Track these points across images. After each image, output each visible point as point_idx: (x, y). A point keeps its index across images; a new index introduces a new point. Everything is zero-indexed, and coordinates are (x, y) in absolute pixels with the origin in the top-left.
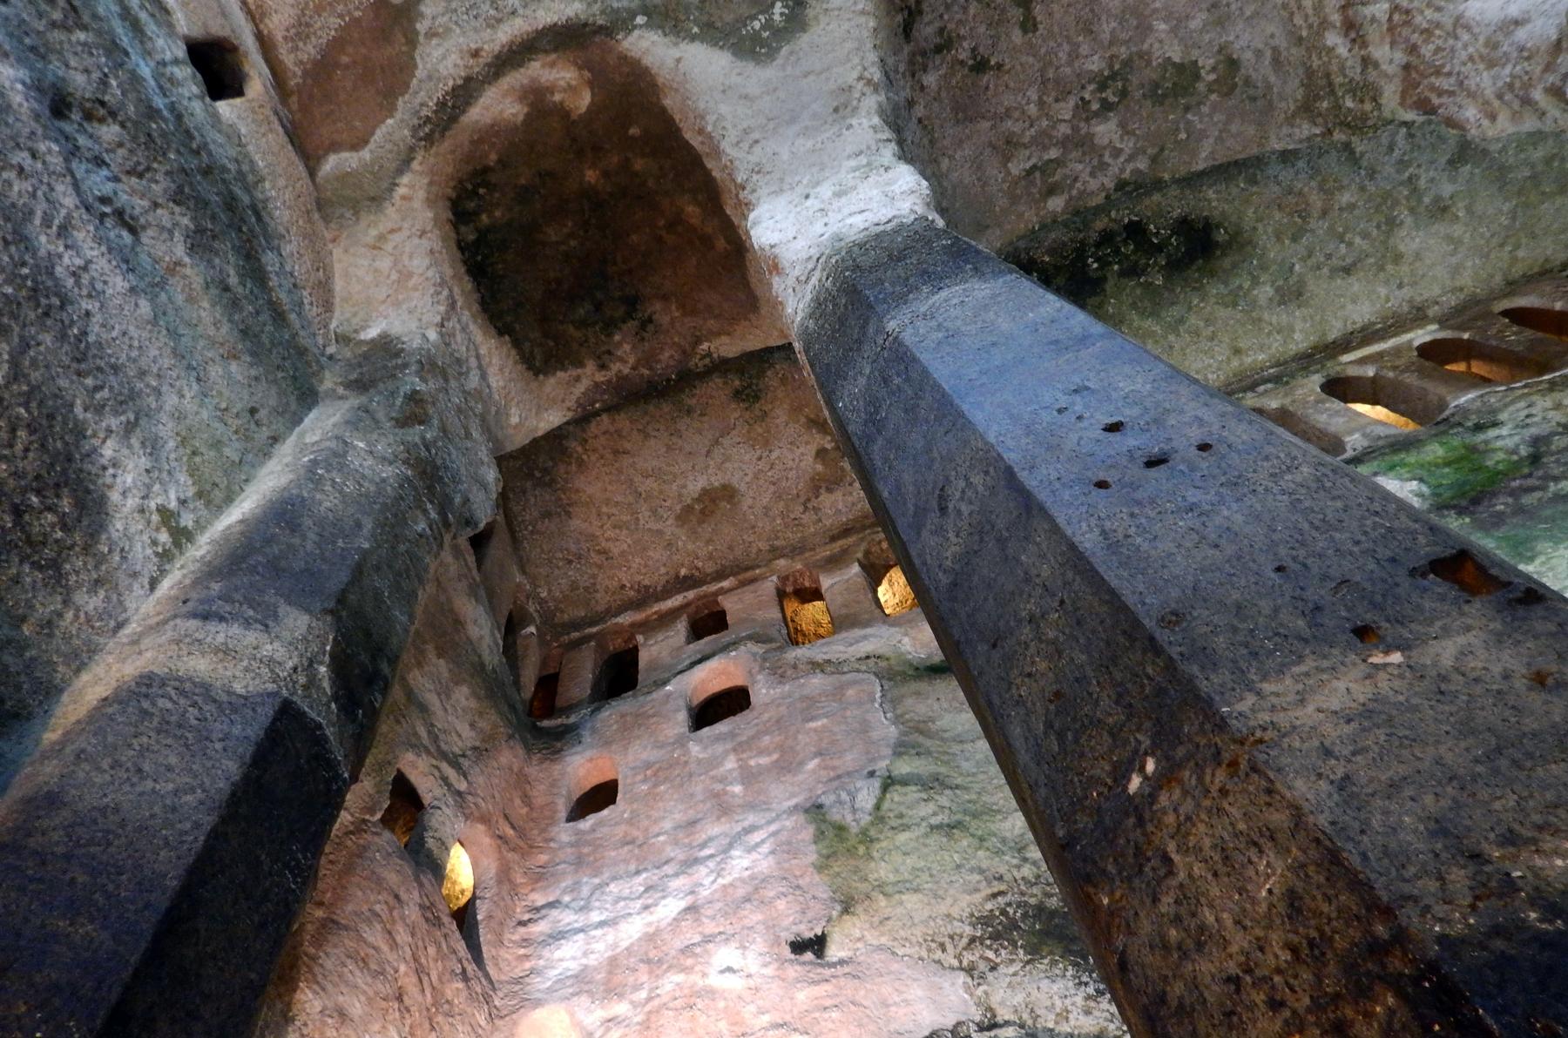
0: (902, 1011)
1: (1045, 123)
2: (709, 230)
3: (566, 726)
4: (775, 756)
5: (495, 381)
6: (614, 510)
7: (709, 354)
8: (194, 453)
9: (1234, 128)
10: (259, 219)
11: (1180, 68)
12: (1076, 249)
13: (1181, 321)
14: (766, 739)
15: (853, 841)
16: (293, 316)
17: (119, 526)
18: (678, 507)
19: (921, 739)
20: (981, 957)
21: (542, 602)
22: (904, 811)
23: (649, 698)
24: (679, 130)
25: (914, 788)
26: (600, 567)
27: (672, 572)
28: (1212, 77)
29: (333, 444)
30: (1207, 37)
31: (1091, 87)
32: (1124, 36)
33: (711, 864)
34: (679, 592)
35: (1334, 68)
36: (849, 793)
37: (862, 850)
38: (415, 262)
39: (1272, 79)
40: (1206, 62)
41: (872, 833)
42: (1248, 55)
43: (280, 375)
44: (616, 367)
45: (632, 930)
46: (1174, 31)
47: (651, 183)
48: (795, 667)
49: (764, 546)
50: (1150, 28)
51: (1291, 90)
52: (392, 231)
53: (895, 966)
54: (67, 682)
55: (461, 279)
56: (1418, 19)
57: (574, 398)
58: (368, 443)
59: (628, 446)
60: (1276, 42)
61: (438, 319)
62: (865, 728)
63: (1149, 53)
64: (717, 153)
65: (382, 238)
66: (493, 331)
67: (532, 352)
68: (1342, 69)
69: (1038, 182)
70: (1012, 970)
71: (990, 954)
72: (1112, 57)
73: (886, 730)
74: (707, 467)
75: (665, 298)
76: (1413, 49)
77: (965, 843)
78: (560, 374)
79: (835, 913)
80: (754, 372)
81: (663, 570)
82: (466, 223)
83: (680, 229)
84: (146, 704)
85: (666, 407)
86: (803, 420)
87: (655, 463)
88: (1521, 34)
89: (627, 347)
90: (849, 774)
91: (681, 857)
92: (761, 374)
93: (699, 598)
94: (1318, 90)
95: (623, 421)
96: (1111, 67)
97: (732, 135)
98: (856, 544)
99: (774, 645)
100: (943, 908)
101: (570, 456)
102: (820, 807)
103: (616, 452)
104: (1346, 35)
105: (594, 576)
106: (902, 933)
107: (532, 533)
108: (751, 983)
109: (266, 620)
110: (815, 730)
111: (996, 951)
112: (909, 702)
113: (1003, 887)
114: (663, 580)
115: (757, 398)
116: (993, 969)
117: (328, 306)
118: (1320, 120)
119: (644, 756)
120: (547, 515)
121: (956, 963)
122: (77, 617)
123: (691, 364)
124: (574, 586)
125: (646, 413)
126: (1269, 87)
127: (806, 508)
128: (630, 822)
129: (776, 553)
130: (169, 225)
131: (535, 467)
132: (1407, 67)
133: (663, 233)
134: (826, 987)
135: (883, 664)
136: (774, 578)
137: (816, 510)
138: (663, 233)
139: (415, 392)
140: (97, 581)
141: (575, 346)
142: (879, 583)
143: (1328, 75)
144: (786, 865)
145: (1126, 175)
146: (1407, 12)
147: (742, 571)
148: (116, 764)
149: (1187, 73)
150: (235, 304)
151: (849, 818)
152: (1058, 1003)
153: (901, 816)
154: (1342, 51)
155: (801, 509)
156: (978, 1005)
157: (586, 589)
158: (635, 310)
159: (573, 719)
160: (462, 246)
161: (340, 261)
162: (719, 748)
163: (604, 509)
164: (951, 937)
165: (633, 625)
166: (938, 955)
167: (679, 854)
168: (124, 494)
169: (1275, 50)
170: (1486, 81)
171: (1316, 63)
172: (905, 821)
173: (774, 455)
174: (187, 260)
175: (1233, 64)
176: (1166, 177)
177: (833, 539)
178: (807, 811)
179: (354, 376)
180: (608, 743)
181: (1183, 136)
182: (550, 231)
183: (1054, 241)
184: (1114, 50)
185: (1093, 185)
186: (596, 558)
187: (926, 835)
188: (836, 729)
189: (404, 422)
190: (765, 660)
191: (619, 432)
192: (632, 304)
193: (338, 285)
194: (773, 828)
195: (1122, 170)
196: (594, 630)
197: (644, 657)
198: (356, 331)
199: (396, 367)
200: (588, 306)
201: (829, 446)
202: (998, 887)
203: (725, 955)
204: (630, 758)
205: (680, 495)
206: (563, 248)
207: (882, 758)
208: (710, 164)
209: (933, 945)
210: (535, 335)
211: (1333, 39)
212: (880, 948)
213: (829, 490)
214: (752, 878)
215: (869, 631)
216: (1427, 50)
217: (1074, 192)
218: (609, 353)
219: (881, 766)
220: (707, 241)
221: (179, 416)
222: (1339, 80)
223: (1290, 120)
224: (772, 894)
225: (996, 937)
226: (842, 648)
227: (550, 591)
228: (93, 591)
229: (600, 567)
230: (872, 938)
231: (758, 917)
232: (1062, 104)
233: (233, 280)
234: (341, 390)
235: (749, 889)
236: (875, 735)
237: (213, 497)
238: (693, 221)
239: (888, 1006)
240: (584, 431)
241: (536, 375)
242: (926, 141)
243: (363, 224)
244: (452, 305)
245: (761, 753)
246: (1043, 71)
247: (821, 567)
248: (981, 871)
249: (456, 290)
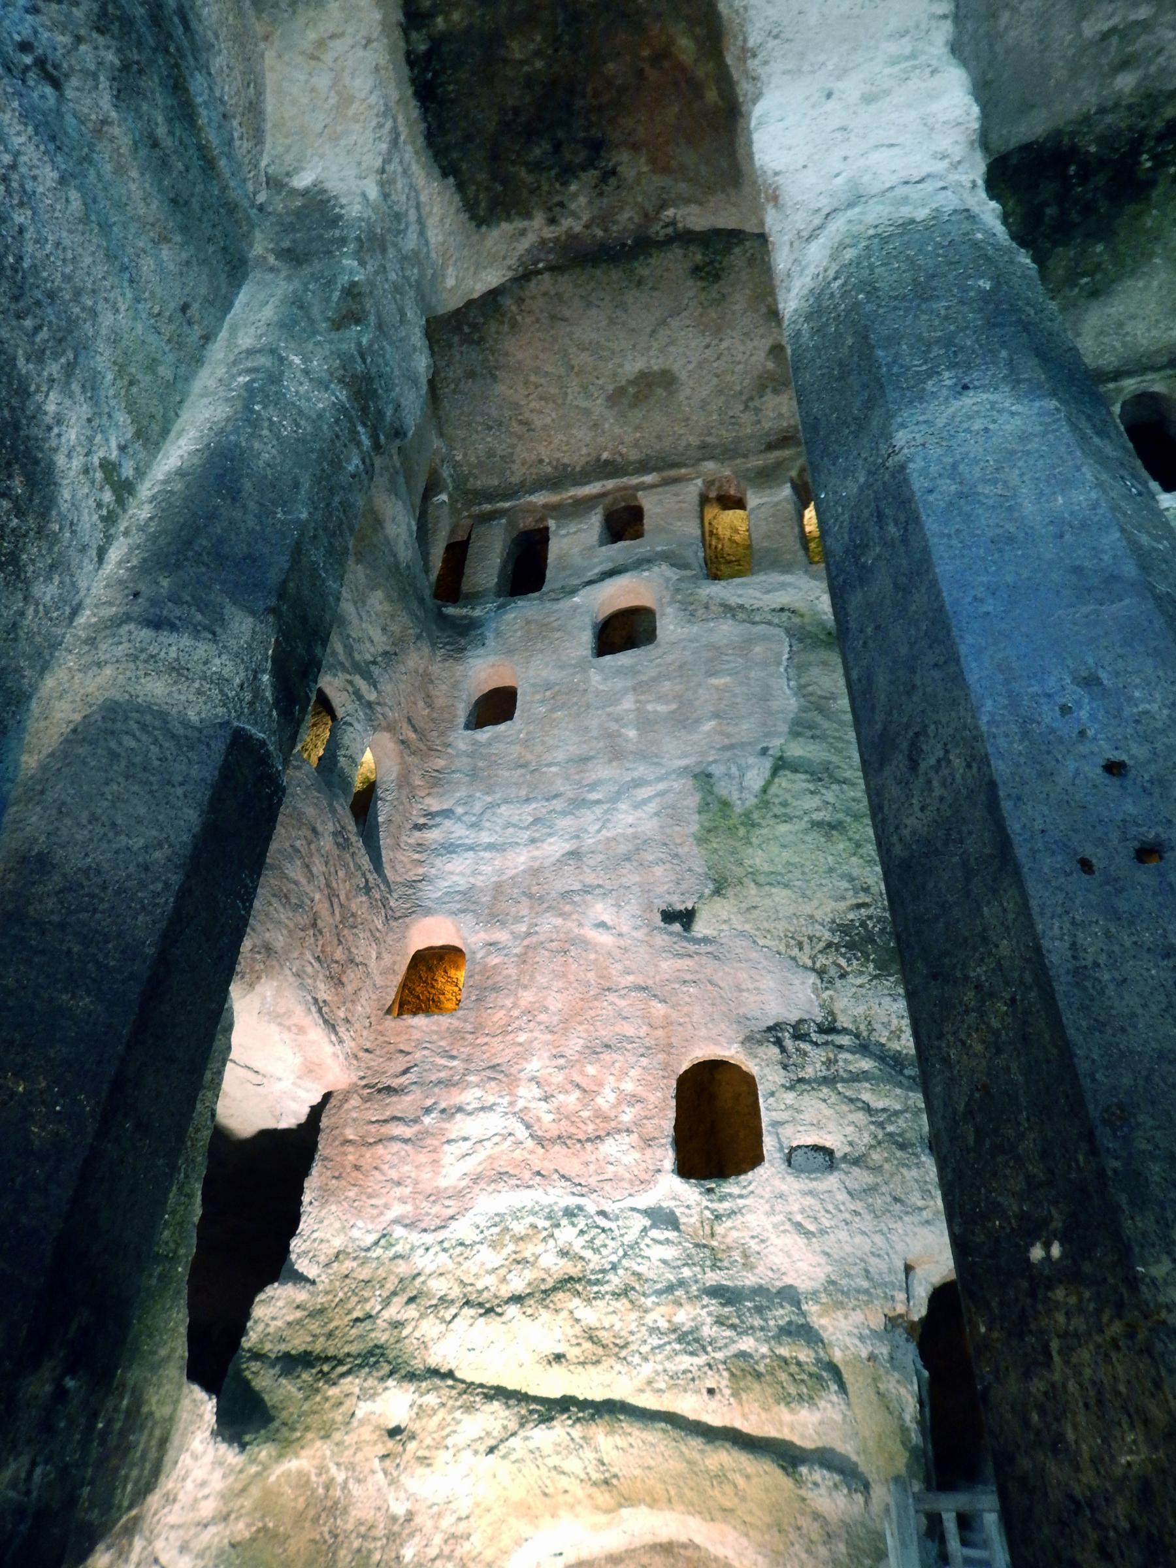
0: (752, 998)
3: (470, 618)
4: (674, 706)
5: (435, 236)
6: (542, 381)
7: (673, 223)
8: (131, 383)
10: (187, 27)
14: (667, 685)
15: (734, 821)
16: (223, 163)
17: (67, 495)
18: (610, 388)
19: (819, 719)
20: (834, 963)
21: (456, 465)
22: (790, 800)
25: (803, 777)
26: (520, 438)
27: (594, 455)
29: (263, 361)
33: (598, 810)
34: (599, 479)
36: (740, 768)
37: (742, 832)
38: (358, 82)
41: (755, 816)
43: (211, 249)
44: (567, 223)
45: (520, 860)
48: (707, 607)
49: (694, 440)
52: (333, 37)
53: (754, 955)
54: (34, 688)
55: (407, 104)
57: (517, 254)
58: (305, 360)
59: (567, 313)
61: (378, 163)
62: (765, 695)
65: (321, 44)
66: (437, 172)
67: (476, 198)
69: (1113, 49)
70: (859, 981)
71: (843, 962)
73: (788, 702)
74: (650, 348)
75: (635, 147)
77: (841, 846)
78: (505, 225)
79: (707, 891)
81: (584, 451)
82: (418, 29)
83: (666, 64)
84: (113, 744)
85: (615, 274)
86: (764, 310)
87: (594, 335)
89: (582, 200)
90: (742, 745)
91: (570, 794)
92: (728, 250)
93: (620, 489)
95: (565, 284)
98: (792, 459)
99: (688, 573)
100: (808, 909)
101: (503, 315)
102: (709, 776)
103: (553, 317)
105: (513, 446)
106: (766, 925)
107: (454, 392)
108: (622, 943)
109: (211, 628)
110: (717, 688)
111: (849, 960)
112: (815, 671)
113: (868, 900)
114: (583, 460)
115: (717, 278)
116: (843, 976)
117: (258, 135)
119: (545, 673)
120: (471, 375)
121: (809, 963)
122: (36, 611)
124: (491, 453)
125: (592, 277)
127: (747, 408)
128: (525, 743)
129: (706, 451)
130: (92, 67)
131: (463, 331)
133: (646, 66)
134: (689, 961)
135: (796, 620)
136: (699, 482)
137: (757, 410)
138: (646, 66)
139: (354, 284)
140: (51, 566)
141: (525, 194)
142: (806, 507)
144: (668, 830)
147: (665, 465)
148: (93, 819)
150: (164, 164)
151: (736, 795)
152: (895, 1022)
153: (785, 804)
155: (742, 408)
156: (822, 1006)
157: (502, 457)
158: (599, 157)
159: (477, 613)
160: (411, 59)
161: (272, 68)
162: (620, 683)
163: (533, 378)
164: (810, 938)
165: (545, 506)
166: (795, 952)
167: (569, 791)
168: (69, 456)
172: (788, 811)
173: (724, 345)
174: (114, 114)
177: (770, 447)
178: (695, 776)
179: (286, 244)
180: (510, 652)
182: (514, 45)
183: (1109, 127)
186: (516, 428)
187: (806, 831)
188: (737, 690)
189: (338, 324)
190: (677, 590)
191: (559, 296)
192: (597, 147)
193: (270, 106)
194: (661, 786)
196: (507, 505)
197: (555, 548)
198: (288, 174)
199: (332, 241)
200: (547, 146)
202: (864, 898)
203: (601, 910)
204: (531, 673)
205: (615, 375)
206: (526, 68)
207: (776, 734)
209: (793, 942)
210: (482, 177)
212: (742, 934)
213: (776, 391)
214: (635, 836)
215: (788, 578)
217: (1153, 69)
218: (561, 204)
219: (776, 743)
220: (697, 88)
221: (115, 340)
224: (651, 858)
225: (851, 946)
226: (758, 594)
227: (465, 455)
228: (49, 579)
229: (520, 438)
230: (737, 923)
231: (636, 878)
233: (161, 131)
234: (271, 259)
235: (631, 847)
236: (775, 705)
237: (151, 433)
239: (741, 990)
240: (522, 288)
241: (478, 226)
243: (301, 20)
244: (395, 143)
245: (659, 699)
247: (749, 480)
248: (851, 879)
249: (400, 118)
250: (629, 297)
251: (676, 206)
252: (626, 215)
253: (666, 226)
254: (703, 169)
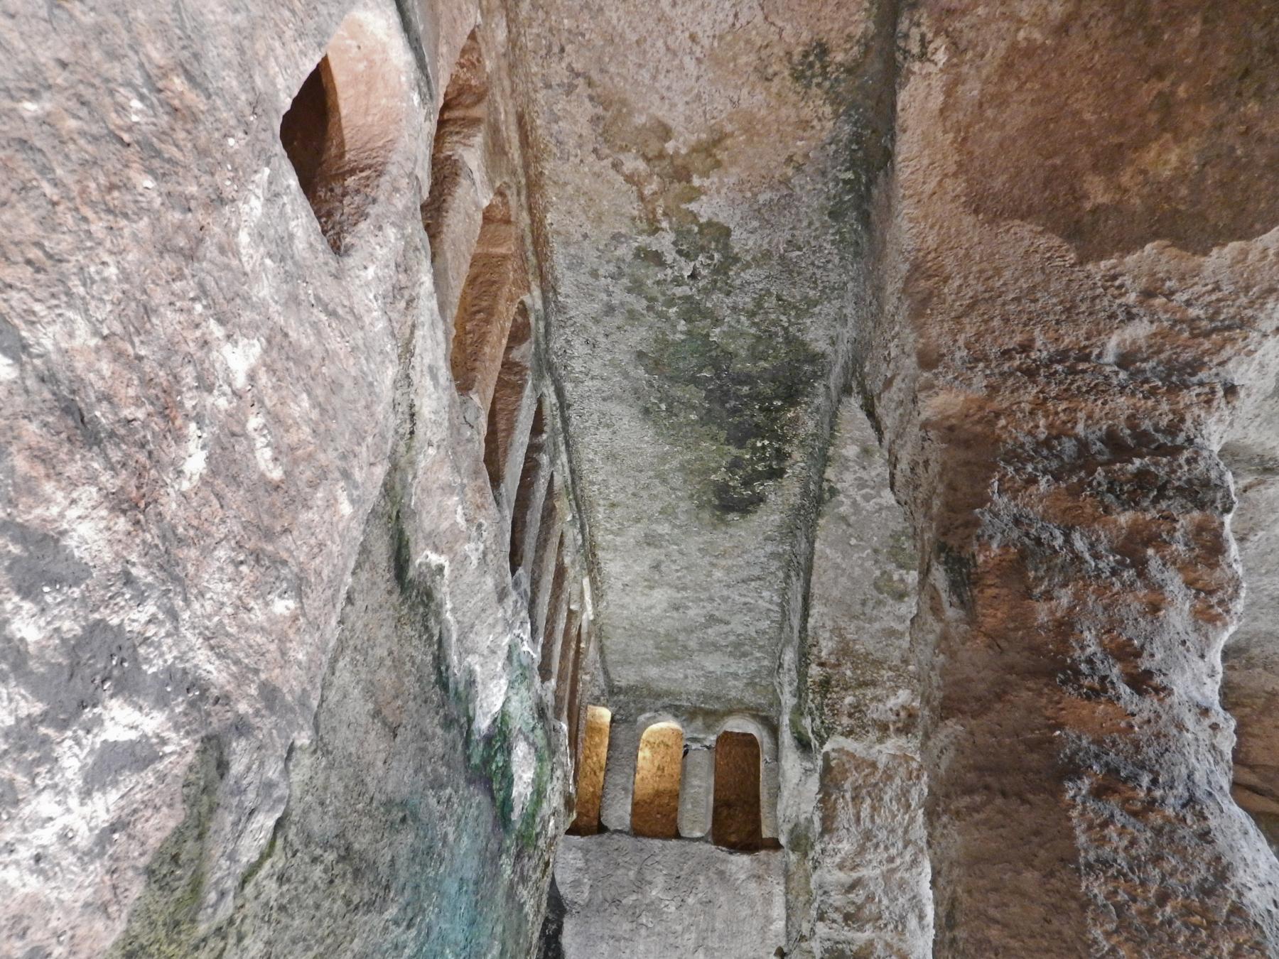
7: (923, 57)
9: (843, 580)
12: (784, 436)
13: (664, 481)
28: (896, 577)
35: (879, 691)
39: (877, 625)
47: (1253, 107)
80: (841, 88)
86: (729, 128)
104: (903, 707)
115: (797, 76)
123: (923, 16)
126: (871, 621)
133: (1164, 85)
145: (841, 497)
176: (821, 522)
181: (853, 542)
185: (849, 477)
195: (847, 496)
201: (670, 147)
222: (870, 692)
223: (837, 631)
251: (949, 65)
254: (995, 136)
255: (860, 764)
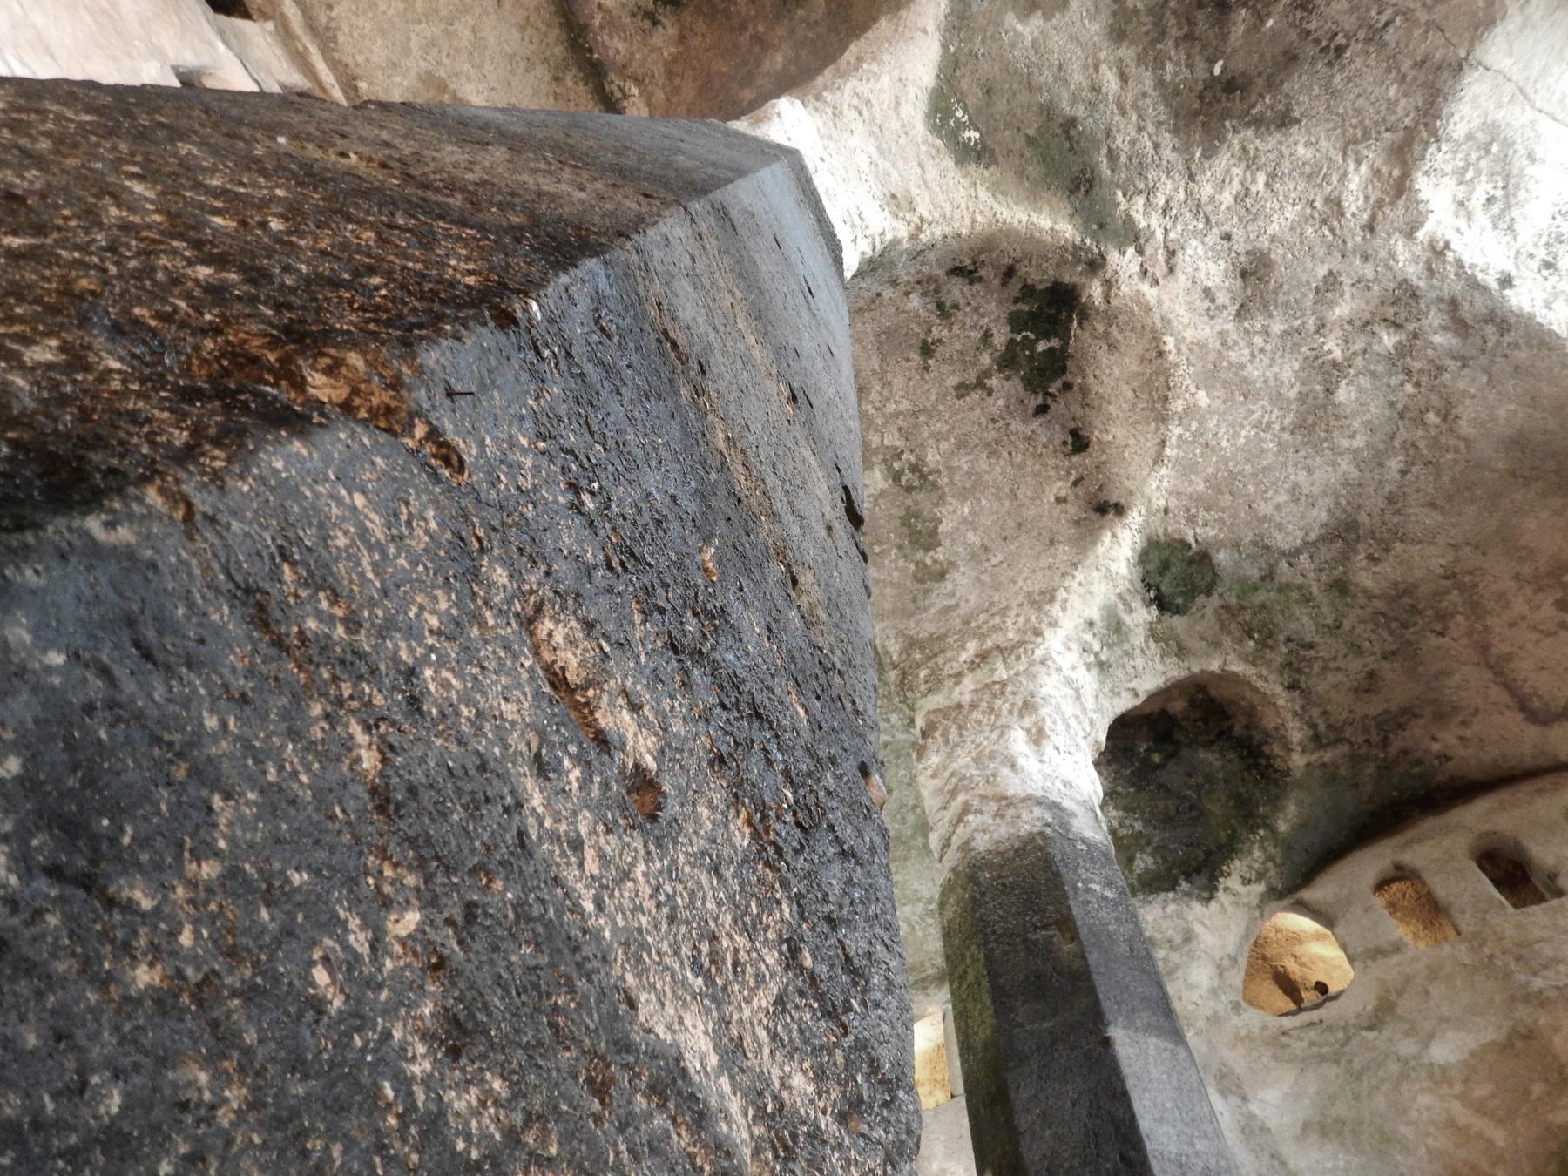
1: (879, 422)
2: (760, 82)
7: (625, 96)
9: (888, 591)
11: (934, 533)
18: (442, 74)
23: (203, 21)
24: (858, 37)
28: (929, 562)
30: (961, 549)
31: (913, 459)
32: (957, 478)
35: (949, 654)
39: (933, 611)
40: (940, 554)
42: (949, 586)
46: (964, 521)
47: (800, 12)
50: (965, 499)
51: (925, 626)
56: (998, 702)
60: (962, 604)
63: (944, 503)
64: (845, 75)
68: (950, 660)
72: (939, 472)
75: (682, 39)
76: (974, 706)
81: (360, 59)
83: (757, 49)
85: (559, 51)
87: (492, 41)
88: (1005, 771)
94: (930, 647)
96: (930, 473)
97: (864, 88)
118: (904, 657)
123: (612, 76)
125: (549, 25)
126: (925, 610)
132: (959, 706)
133: (751, 31)
143: (943, 651)
146: (1002, 693)
149: (929, 540)
154: (964, 656)
165: (283, 16)
169: (957, 606)
170: (962, 761)
171: (951, 640)
175: (941, 576)
184: (944, 472)
205: (457, 75)
208: (828, 72)
211: (972, 647)
216: (976, 715)
220: (748, 80)
222: (940, 660)
223: (901, 633)
232: (897, 434)
238: (767, 65)
242: (861, 303)
246: (924, 410)
250: (540, 71)
251: (641, 95)
252: (621, 46)
253: (621, 90)
255: (944, 713)
